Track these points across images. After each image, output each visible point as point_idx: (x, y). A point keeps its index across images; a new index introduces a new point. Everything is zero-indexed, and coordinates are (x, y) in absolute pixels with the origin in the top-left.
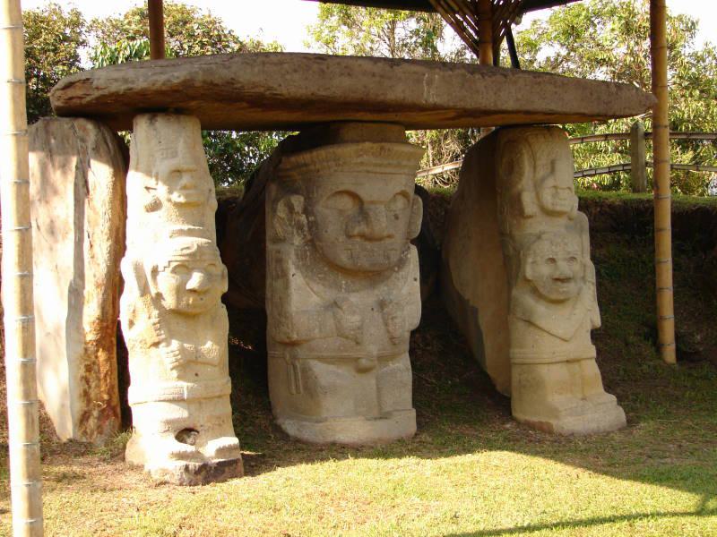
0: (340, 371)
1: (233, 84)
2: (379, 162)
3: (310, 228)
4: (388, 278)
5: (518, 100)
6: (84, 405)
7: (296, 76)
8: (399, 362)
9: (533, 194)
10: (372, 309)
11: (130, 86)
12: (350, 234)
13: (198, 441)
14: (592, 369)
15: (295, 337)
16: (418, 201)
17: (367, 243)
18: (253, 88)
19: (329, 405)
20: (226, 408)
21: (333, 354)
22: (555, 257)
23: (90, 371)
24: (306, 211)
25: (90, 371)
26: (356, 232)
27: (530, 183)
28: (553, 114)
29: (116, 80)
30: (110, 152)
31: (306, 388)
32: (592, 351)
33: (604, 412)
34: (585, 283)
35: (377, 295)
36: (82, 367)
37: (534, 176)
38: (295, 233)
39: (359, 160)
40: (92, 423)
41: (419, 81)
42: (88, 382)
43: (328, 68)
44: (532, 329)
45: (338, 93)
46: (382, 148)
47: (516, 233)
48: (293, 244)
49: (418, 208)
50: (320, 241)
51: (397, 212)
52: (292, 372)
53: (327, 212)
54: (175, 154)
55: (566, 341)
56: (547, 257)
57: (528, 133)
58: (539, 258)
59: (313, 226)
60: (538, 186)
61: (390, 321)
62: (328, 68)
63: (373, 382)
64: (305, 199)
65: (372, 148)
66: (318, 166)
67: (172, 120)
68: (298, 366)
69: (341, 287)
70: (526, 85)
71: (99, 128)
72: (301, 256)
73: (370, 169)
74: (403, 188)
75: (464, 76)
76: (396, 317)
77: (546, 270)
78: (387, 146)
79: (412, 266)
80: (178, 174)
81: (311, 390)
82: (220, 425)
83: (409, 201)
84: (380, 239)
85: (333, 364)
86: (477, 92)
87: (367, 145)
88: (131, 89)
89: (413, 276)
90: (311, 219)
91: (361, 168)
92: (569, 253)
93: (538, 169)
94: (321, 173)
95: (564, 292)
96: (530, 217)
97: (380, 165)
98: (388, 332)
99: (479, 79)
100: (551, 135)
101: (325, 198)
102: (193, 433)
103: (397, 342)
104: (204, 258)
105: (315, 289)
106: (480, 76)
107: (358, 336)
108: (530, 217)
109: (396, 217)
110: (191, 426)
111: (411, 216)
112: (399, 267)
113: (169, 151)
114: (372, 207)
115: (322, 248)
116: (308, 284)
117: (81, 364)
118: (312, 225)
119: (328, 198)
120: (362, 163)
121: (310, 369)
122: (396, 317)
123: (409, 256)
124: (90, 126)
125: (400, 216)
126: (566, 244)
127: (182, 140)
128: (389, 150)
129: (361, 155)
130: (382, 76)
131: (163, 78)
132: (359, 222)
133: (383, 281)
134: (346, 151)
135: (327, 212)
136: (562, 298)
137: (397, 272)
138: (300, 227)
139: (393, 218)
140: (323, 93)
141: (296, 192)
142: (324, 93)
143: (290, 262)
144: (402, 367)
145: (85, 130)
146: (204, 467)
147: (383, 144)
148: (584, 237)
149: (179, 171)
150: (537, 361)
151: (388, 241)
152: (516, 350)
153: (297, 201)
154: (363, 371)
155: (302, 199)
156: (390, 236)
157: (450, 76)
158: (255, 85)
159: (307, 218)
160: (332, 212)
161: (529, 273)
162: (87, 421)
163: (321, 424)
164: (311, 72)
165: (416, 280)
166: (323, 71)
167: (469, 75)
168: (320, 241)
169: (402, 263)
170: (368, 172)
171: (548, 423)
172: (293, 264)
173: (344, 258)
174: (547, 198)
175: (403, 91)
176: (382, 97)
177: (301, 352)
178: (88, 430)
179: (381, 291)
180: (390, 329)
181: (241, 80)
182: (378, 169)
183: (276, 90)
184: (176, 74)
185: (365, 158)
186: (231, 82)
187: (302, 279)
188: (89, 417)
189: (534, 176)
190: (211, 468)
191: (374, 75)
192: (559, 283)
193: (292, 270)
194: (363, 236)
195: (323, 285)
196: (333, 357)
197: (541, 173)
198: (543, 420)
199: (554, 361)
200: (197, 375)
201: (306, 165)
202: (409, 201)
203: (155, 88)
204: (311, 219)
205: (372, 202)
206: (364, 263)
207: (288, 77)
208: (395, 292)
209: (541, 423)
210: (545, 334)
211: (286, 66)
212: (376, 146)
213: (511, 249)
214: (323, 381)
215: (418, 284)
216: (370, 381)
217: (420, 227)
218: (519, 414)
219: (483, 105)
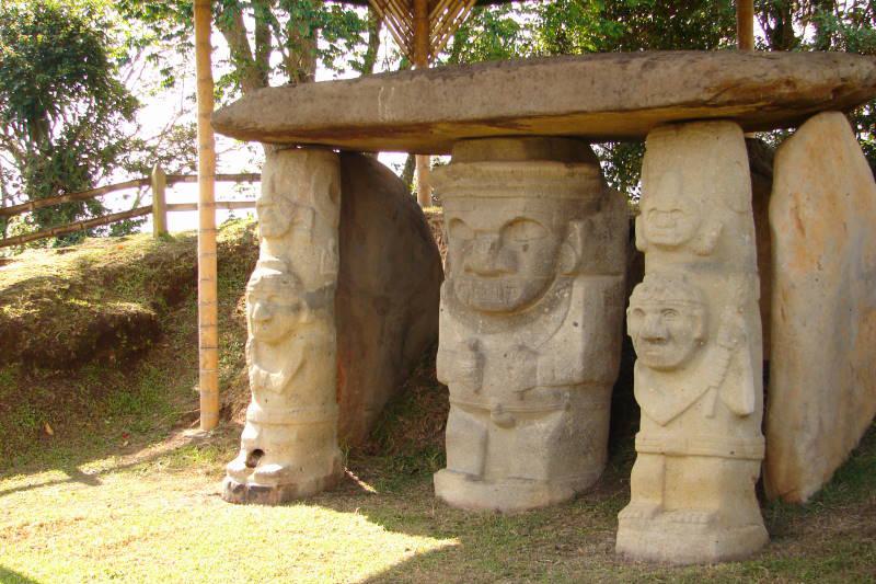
4: (533, 320)
5: (483, 104)
28: (530, 117)
41: (374, 97)
49: (575, 237)
51: (530, 243)
69: (478, 328)
70: (495, 84)
74: (520, 214)
78: (477, 166)
79: (572, 307)
86: (436, 101)
89: (573, 320)
92: (661, 303)
97: (481, 189)
99: (439, 84)
125: (531, 246)
130: (340, 97)
137: (547, 314)
165: (576, 325)
175: (358, 112)
179: (523, 334)
182: (482, 194)
185: (462, 182)
193: (441, 306)
212: (468, 166)
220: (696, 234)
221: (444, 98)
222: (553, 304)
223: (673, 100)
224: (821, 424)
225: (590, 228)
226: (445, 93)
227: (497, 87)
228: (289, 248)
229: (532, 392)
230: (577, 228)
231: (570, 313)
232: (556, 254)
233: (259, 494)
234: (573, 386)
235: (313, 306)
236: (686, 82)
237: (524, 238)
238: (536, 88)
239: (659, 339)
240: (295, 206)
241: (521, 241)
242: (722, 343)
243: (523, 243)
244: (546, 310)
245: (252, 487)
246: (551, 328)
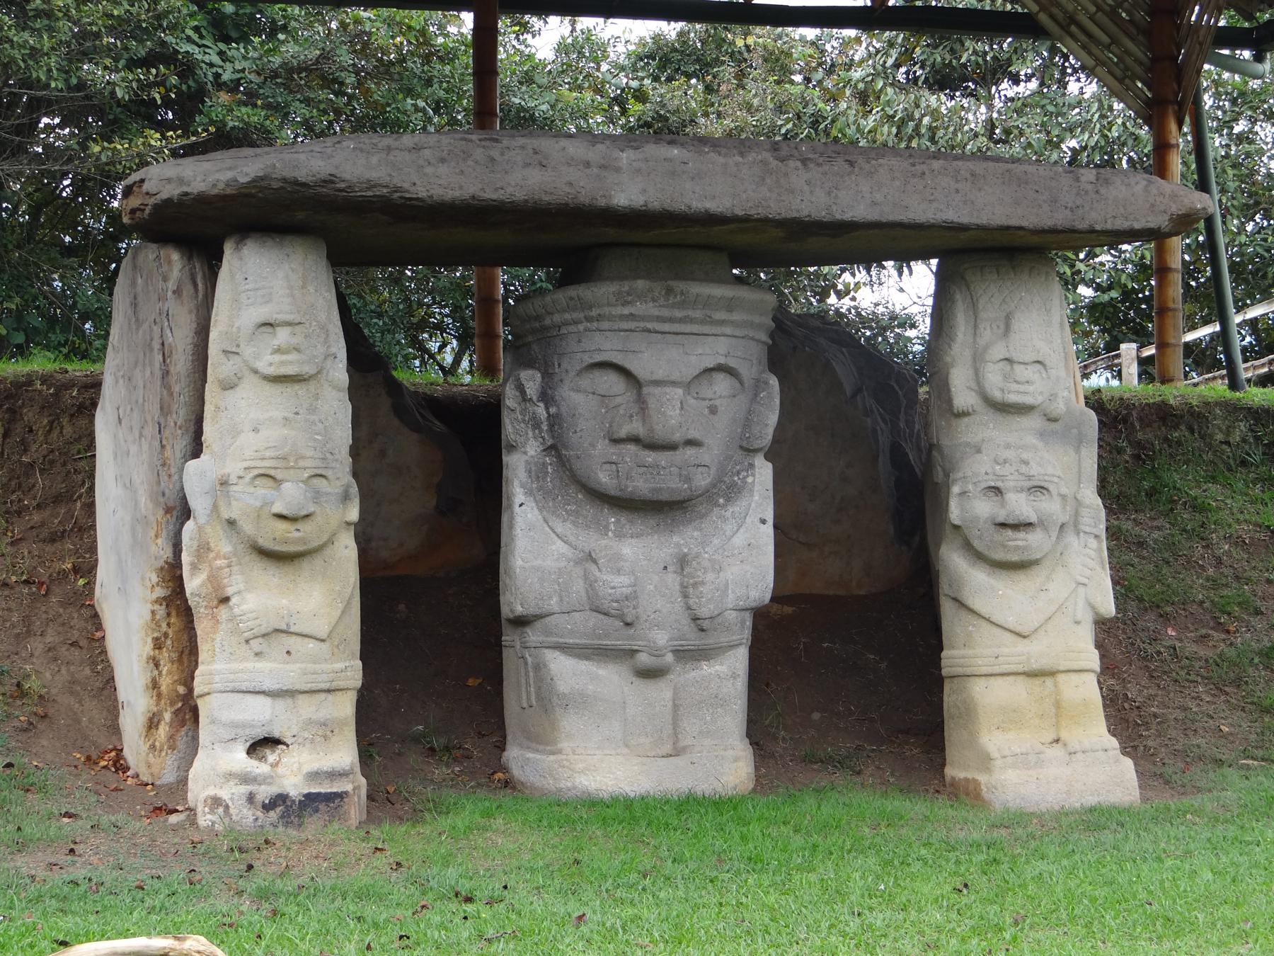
0: (601, 672)
1: (333, 182)
2: (666, 313)
3: (551, 426)
4: (703, 516)
5: (874, 203)
6: (153, 702)
7: (443, 169)
8: (722, 664)
9: (971, 372)
10: (665, 568)
11: (185, 189)
12: (615, 437)
13: (284, 760)
14: (1086, 690)
15: (519, 610)
16: (766, 383)
17: (647, 452)
18: (368, 189)
19: (570, 723)
20: (345, 707)
21: (583, 641)
22: (999, 484)
23: (160, 648)
24: (546, 397)
25: (160, 648)
26: (623, 433)
27: (968, 353)
29: (169, 180)
30: (197, 297)
31: (540, 698)
32: (1093, 659)
33: (1095, 768)
34: (1078, 534)
35: (678, 545)
36: (149, 640)
37: (975, 341)
38: (530, 434)
39: (626, 311)
40: (163, 731)
42: (157, 665)
43: (502, 154)
44: (963, 614)
45: (520, 195)
46: (669, 291)
47: (945, 442)
48: (525, 453)
50: (566, 448)
51: (717, 402)
52: (523, 671)
53: (578, 398)
54: (268, 300)
55: (1024, 637)
56: (984, 485)
57: (966, 266)
58: (970, 487)
59: (554, 421)
60: (978, 359)
61: (691, 590)
62: (502, 154)
63: (668, 694)
64: (543, 378)
65: (651, 290)
66: (557, 318)
67: (270, 243)
68: (530, 660)
69: (607, 528)
71: (190, 258)
72: (537, 474)
73: (650, 326)
74: (722, 360)
75: (764, 163)
76: (703, 583)
77: (983, 508)
78: (679, 285)
80: (270, 329)
81: (546, 700)
82: (325, 738)
83: (741, 383)
84: (672, 447)
85: (587, 658)
87: (641, 284)
88: (186, 194)
90: (553, 410)
91: (632, 325)
92: (1030, 477)
93: (981, 326)
94: (564, 331)
95: (1017, 548)
96: (965, 414)
97: (671, 320)
98: (689, 608)
100: (1013, 268)
101: (572, 374)
102: (280, 746)
103: (706, 624)
104: (301, 463)
105: (559, 530)
106: (799, 164)
107: (626, 611)
108: (965, 414)
109: (713, 410)
110: (276, 735)
111: (749, 412)
112: (728, 500)
113: (260, 293)
114: (657, 390)
115: (568, 460)
116: (546, 521)
117: (147, 635)
118: (554, 421)
119: (579, 373)
120: (632, 317)
121: (545, 666)
122: (703, 583)
123: (750, 480)
124: (175, 256)
126: (1026, 463)
127: (281, 274)
128: (682, 293)
129: (629, 303)
130: (603, 167)
131: (229, 175)
132: (631, 416)
133: (690, 521)
134: (601, 292)
135: (578, 398)
136: (1014, 557)
137: (723, 506)
138: (536, 425)
139: (706, 411)
140: (490, 195)
141: (530, 364)
142: (494, 196)
143: (516, 483)
144: (729, 672)
145: (170, 262)
146: (280, 800)
147: (670, 283)
148: (1084, 452)
149: (271, 325)
150: (968, 671)
151: (690, 452)
152: (955, 652)
153: (532, 381)
154: (650, 674)
155: (538, 376)
156: (691, 443)
157: (737, 164)
158: (372, 185)
159: (547, 408)
160: (584, 399)
161: (955, 512)
162: (157, 727)
163: (552, 758)
164: (470, 163)
165: (763, 522)
166: (493, 160)
167: (774, 163)
168: (566, 448)
169: (726, 489)
170: (649, 331)
171: (975, 781)
172: (522, 486)
173: (604, 479)
174: (994, 380)
176: (602, 202)
177: (533, 635)
178: (157, 744)
179: (685, 538)
180: (691, 602)
181: (347, 176)
182: (666, 327)
183: (408, 191)
184: (245, 169)
185: (639, 308)
186: (329, 181)
187: (536, 512)
188: (159, 722)
189: (975, 341)
190: (294, 801)
191: (587, 164)
192: (1009, 533)
194: (635, 440)
195: (573, 523)
196: (586, 647)
197: (986, 334)
198: (970, 776)
199: (997, 670)
200: (288, 652)
201: (538, 318)
202: (741, 383)
203: (215, 191)
204: (553, 410)
205: (657, 383)
206: (641, 486)
207: (429, 170)
208: (716, 541)
209: (967, 780)
210: (984, 624)
211: (427, 152)
213: (941, 474)
214: (563, 686)
215: (768, 530)
216: (661, 692)
217: (770, 431)
218: (949, 771)
219: (805, 213)
220: (1053, 397)
221: (806, 188)
223: (1137, 226)
224: (963, 657)
226: (808, 183)
227: (898, 183)
228: (317, 397)
229: (720, 620)
231: (753, 505)
233: (322, 807)
236: (1153, 205)
237: (710, 396)
238: (957, 191)
239: (1028, 525)
241: (704, 399)
242: (1088, 529)
243: (707, 403)
244: (721, 501)
245: (309, 797)
246: (729, 528)
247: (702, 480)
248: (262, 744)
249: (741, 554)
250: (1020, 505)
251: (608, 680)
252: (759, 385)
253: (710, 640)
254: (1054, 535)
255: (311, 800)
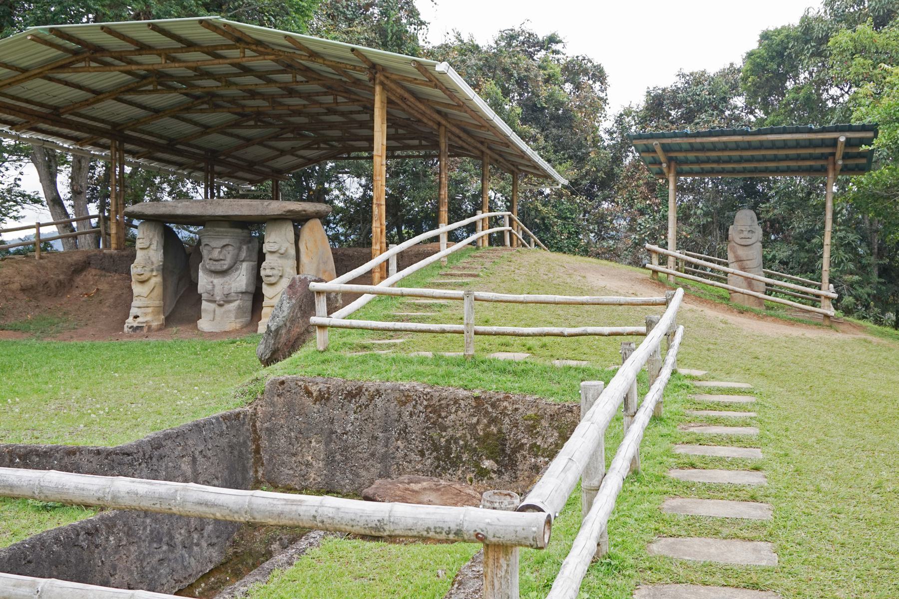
179: (227, 278)
206: (213, 268)
216: (223, 309)
222: (237, 269)
225: (248, 248)
230: (245, 247)
232: (238, 255)
234: (242, 293)
235: (157, 270)
240: (151, 240)
247: (225, 267)
248: (136, 317)
249: (241, 280)
250: (268, 272)
251: (213, 306)
252: (240, 249)
253: (229, 299)
254: (277, 278)
255: (138, 327)
